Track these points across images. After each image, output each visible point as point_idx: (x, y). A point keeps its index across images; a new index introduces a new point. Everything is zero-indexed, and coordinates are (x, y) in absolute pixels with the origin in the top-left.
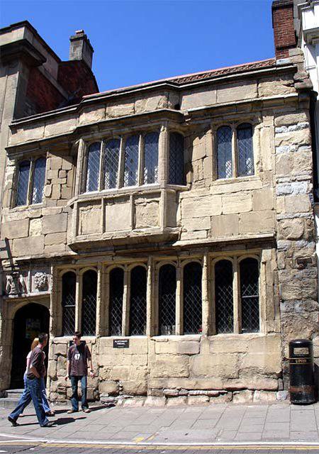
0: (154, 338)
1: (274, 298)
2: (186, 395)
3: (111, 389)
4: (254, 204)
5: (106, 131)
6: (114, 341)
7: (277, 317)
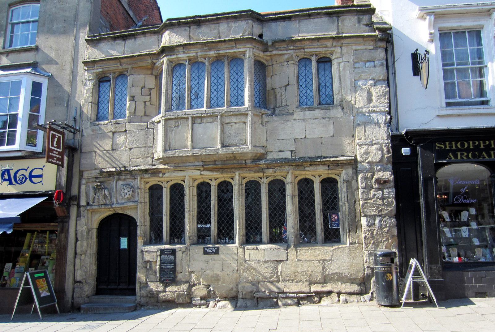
5: (192, 53)
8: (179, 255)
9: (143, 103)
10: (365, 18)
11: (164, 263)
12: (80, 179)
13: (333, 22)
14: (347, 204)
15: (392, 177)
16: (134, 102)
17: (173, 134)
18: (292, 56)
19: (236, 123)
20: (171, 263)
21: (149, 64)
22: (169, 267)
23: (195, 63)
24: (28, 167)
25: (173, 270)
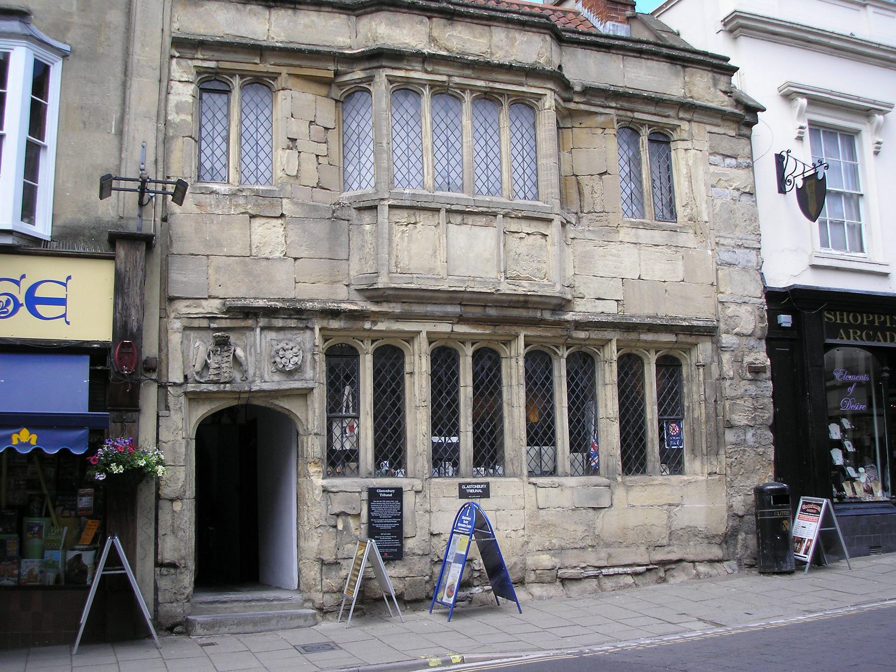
0: (533, 480)
2: (596, 577)
4: (686, 271)
6: (460, 485)
7: (722, 452)
8: (409, 499)
10: (723, 79)
11: (378, 517)
12: (164, 316)
13: (677, 75)
14: (703, 405)
15: (768, 362)
17: (406, 239)
19: (528, 234)
20: (393, 517)
21: (331, 75)
22: (388, 527)
24: (23, 276)
25: (398, 532)
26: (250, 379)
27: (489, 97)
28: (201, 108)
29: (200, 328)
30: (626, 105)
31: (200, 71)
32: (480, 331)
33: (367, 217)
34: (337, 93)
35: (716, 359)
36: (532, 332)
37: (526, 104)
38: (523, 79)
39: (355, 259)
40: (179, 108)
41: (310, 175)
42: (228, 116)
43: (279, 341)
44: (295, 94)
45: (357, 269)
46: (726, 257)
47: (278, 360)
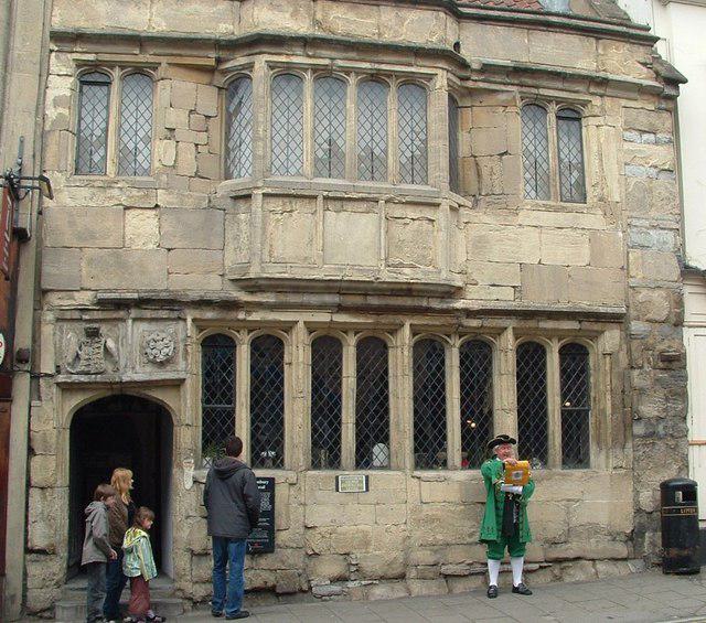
0: (417, 473)
1: (624, 414)
3: (336, 569)
7: (629, 445)
8: (281, 491)
9: (193, 148)
12: (38, 306)
16: (173, 143)
18: (514, 97)
21: (212, 62)
23: (322, 74)
26: (121, 370)
27: (376, 78)
28: (80, 101)
29: (72, 320)
30: (529, 82)
31: (79, 64)
32: (361, 320)
33: (242, 205)
34: (221, 80)
35: (624, 347)
36: (418, 321)
37: (415, 85)
38: (412, 60)
39: (230, 247)
40: (57, 102)
41: (188, 163)
42: (107, 107)
43: (151, 333)
44: (175, 83)
45: (232, 258)
46: (637, 238)
47: (149, 351)
